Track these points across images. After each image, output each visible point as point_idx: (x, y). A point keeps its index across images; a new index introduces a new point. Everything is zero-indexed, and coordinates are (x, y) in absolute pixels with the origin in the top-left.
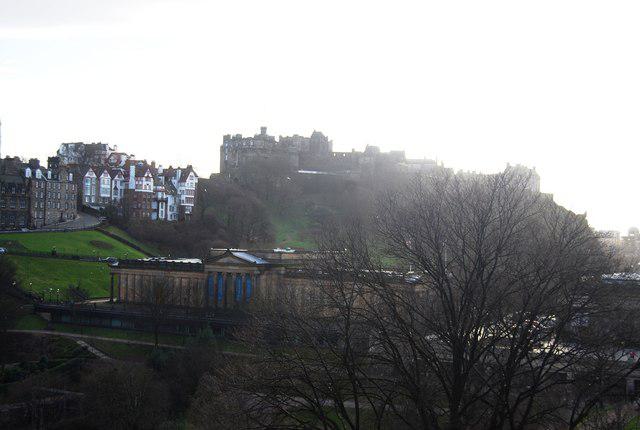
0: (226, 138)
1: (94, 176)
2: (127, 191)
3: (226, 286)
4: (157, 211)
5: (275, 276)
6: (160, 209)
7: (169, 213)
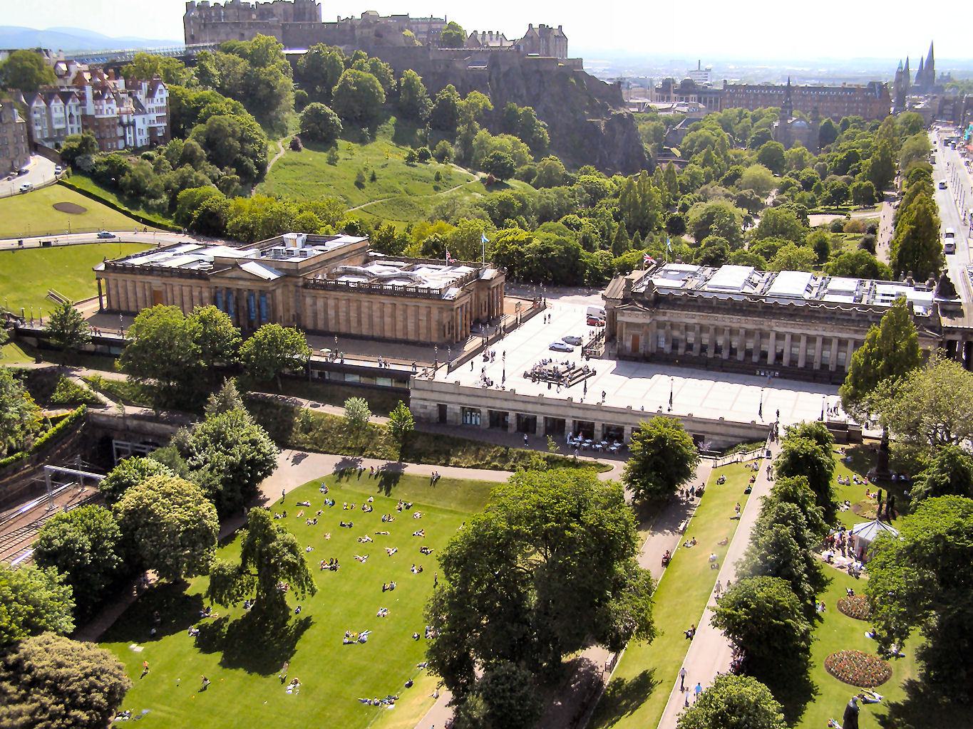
0: (189, 6)
1: (43, 104)
2: (85, 117)
3: (237, 300)
4: (124, 137)
5: (292, 288)
6: (128, 136)
7: (139, 138)
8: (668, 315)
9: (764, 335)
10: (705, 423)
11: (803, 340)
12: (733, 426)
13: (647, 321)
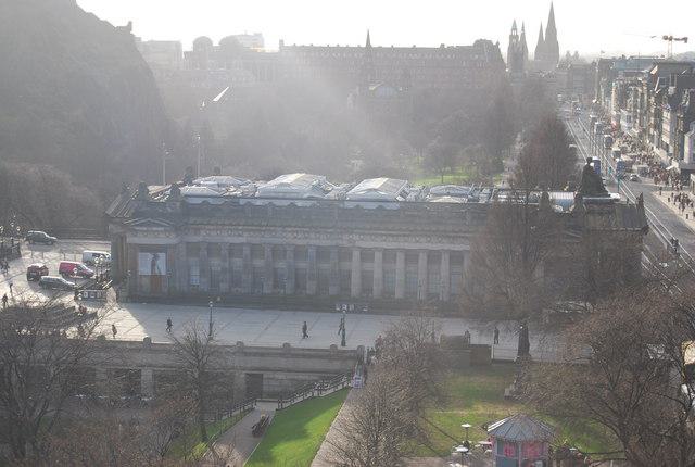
8: (203, 233)
9: (344, 254)
10: (262, 355)
11: (401, 257)
12: (304, 356)
13: (172, 240)
